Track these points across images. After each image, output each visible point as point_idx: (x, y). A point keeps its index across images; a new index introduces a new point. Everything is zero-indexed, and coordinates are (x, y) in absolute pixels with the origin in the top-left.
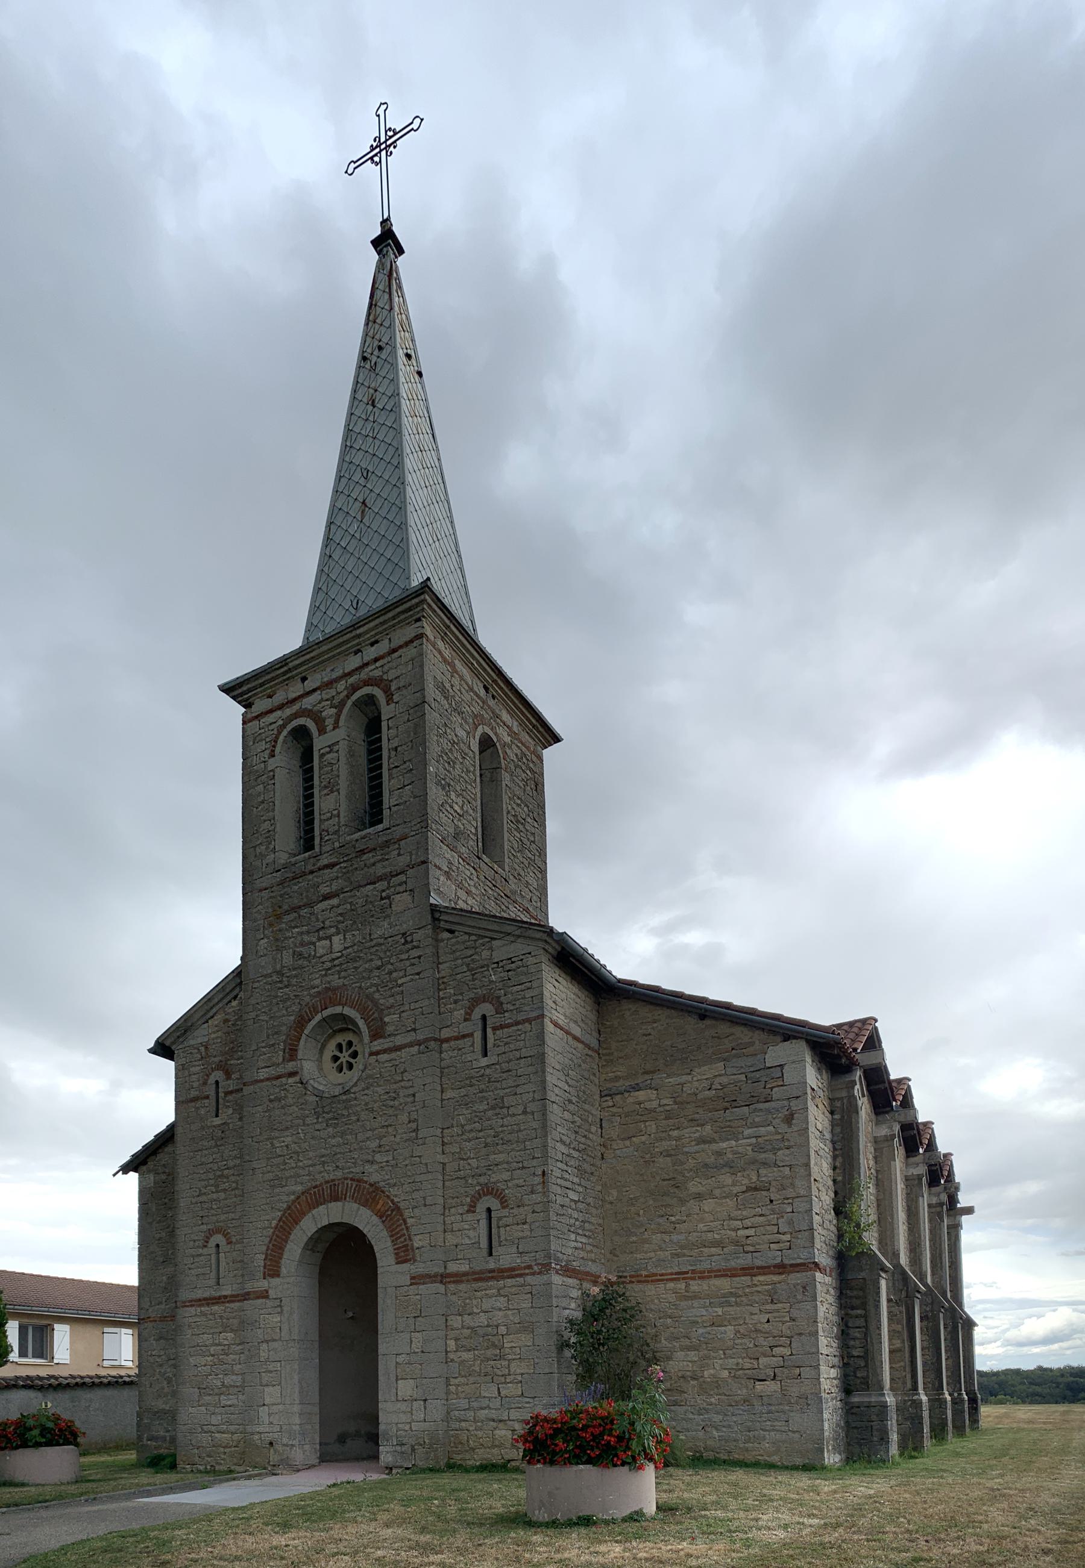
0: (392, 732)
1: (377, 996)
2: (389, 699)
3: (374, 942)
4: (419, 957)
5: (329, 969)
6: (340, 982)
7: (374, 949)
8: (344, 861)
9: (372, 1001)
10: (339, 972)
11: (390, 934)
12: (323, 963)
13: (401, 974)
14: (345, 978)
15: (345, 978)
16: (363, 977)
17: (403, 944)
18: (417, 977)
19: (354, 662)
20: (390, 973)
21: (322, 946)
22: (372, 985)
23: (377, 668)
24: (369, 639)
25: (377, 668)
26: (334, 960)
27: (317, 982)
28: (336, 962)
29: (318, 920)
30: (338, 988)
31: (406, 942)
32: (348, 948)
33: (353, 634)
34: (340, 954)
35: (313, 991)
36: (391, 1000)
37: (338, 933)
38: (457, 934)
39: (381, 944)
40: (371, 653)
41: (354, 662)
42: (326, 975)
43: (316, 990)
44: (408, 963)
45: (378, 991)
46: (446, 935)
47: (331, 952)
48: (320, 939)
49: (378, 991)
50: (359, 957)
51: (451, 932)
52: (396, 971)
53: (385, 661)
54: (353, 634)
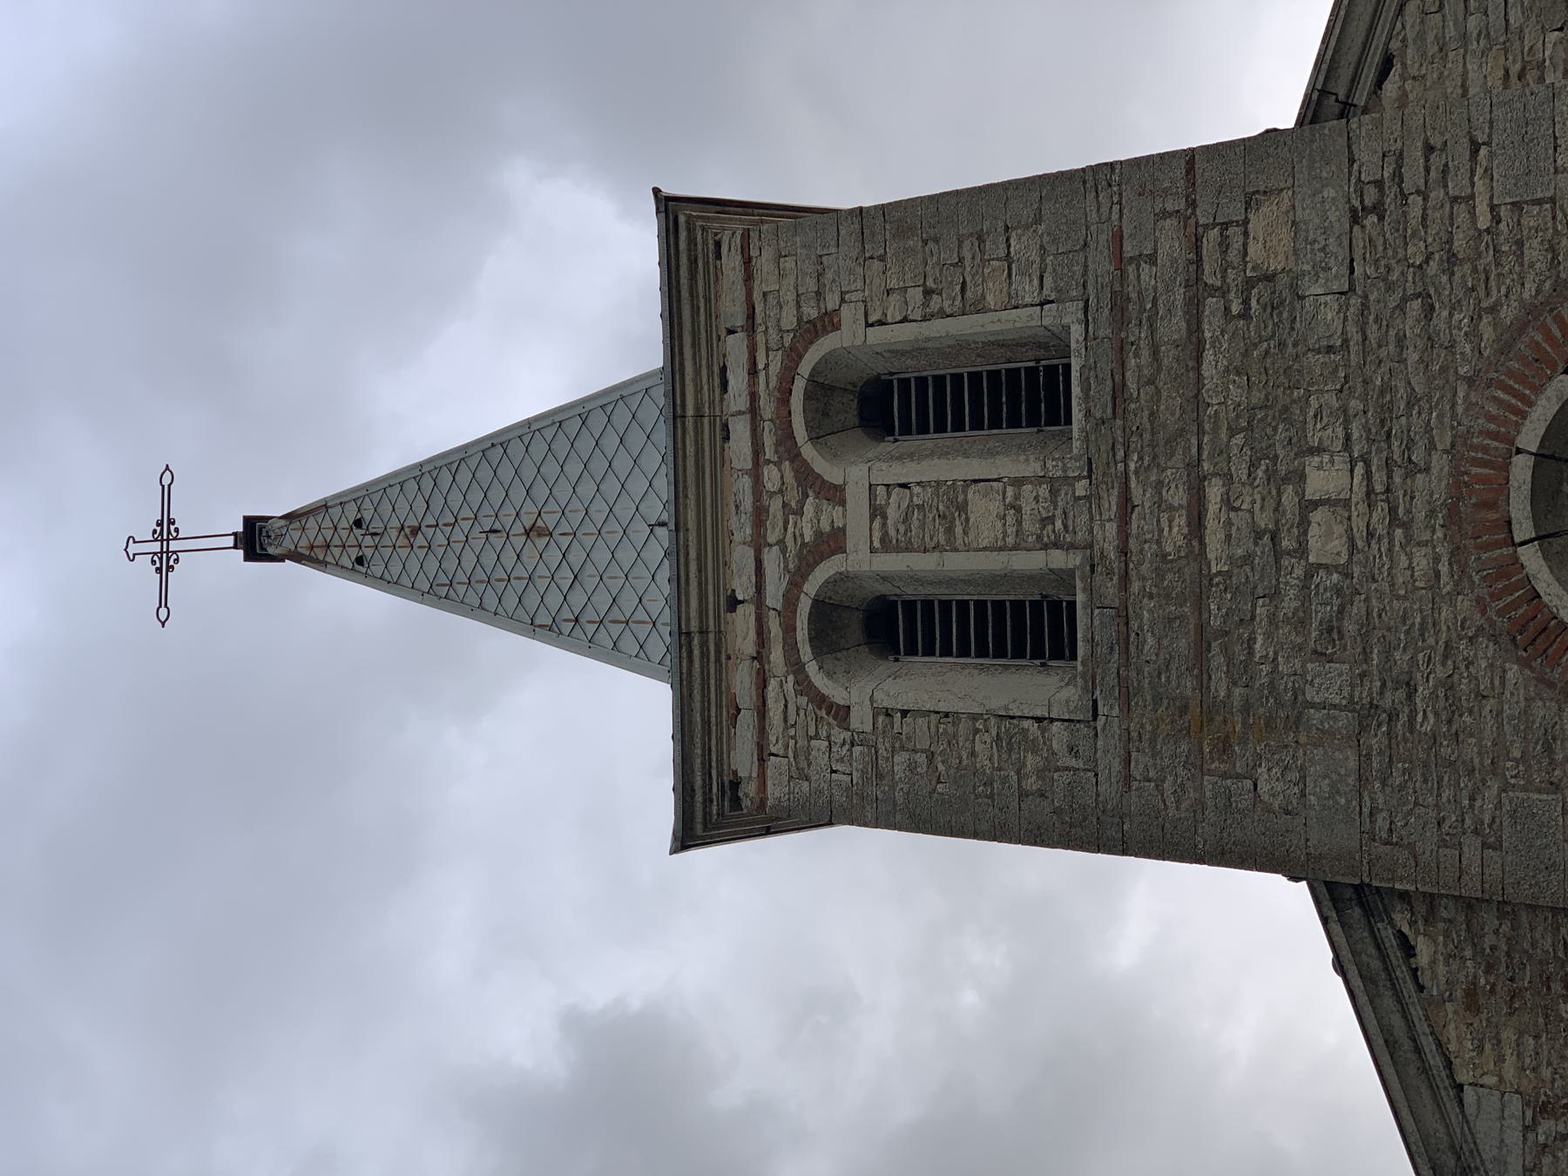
0: (893, 314)
1: (1508, 313)
2: (829, 322)
3: (1352, 329)
4: (1429, 149)
5: (1393, 510)
6: (1440, 462)
7: (1373, 333)
8: (1125, 460)
9: (1522, 330)
10: (1412, 470)
11: (1345, 271)
12: (1370, 534)
13: (1462, 216)
14: (1431, 447)
15: (1431, 447)
16: (1443, 369)
17: (1381, 218)
18: (1483, 151)
19: (740, 430)
20: (1452, 259)
21: (1326, 542)
22: (1474, 334)
23: (767, 366)
24: (711, 390)
25: (767, 366)
26: (1370, 492)
27: (1421, 562)
28: (1379, 479)
29: (1248, 558)
30: (1456, 473)
31: (1378, 209)
32: (1348, 438)
33: (690, 423)
34: (1359, 469)
35: (1444, 578)
36: (1534, 251)
37: (1302, 477)
38: (1395, 45)
39: (1365, 306)
40: (738, 380)
41: (740, 430)
42: (1406, 526)
43: (1444, 568)
44: (1437, 195)
45: (1493, 310)
46: (1391, 87)
47: (1347, 503)
48: (1302, 550)
49: (1493, 310)
50: (1382, 393)
51: (1387, 64)
52: (1450, 241)
53: (760, 338)
54: (690, 423)
